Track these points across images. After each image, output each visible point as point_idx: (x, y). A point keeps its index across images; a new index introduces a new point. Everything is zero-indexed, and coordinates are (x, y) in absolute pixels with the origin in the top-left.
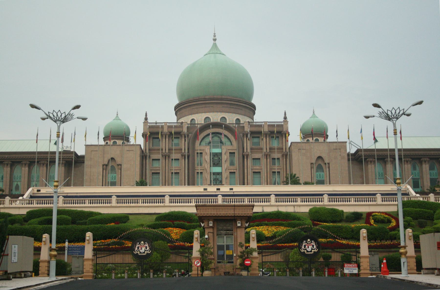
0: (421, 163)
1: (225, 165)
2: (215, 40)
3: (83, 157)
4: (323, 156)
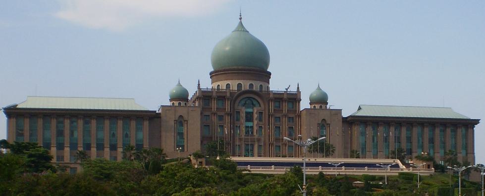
1: (256, 122)
4: (326, 118)
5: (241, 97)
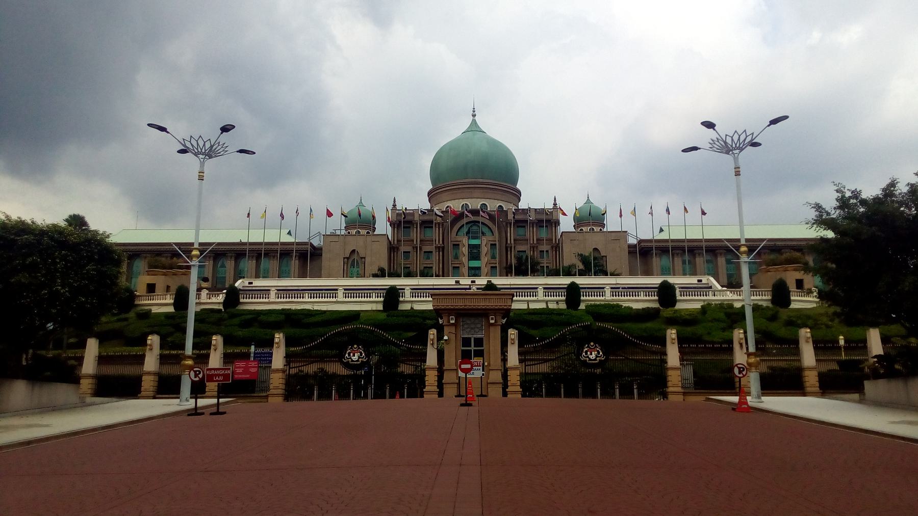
0: (716, 256)
2: (474, 116)
3: (320, 249)
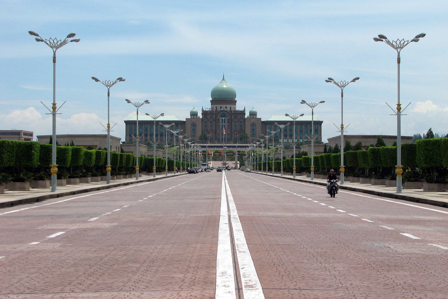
2: (224, 77)
4: (254, 122)
5: (221, 113)
